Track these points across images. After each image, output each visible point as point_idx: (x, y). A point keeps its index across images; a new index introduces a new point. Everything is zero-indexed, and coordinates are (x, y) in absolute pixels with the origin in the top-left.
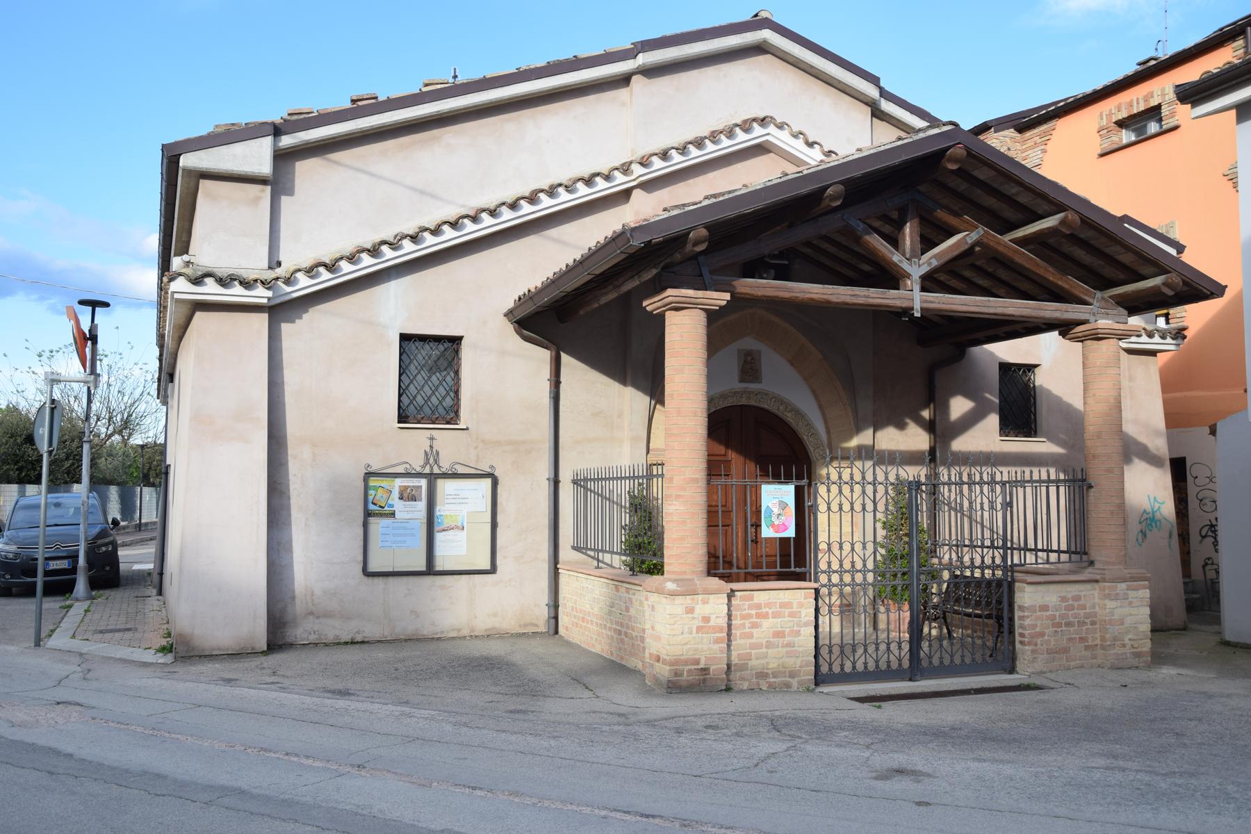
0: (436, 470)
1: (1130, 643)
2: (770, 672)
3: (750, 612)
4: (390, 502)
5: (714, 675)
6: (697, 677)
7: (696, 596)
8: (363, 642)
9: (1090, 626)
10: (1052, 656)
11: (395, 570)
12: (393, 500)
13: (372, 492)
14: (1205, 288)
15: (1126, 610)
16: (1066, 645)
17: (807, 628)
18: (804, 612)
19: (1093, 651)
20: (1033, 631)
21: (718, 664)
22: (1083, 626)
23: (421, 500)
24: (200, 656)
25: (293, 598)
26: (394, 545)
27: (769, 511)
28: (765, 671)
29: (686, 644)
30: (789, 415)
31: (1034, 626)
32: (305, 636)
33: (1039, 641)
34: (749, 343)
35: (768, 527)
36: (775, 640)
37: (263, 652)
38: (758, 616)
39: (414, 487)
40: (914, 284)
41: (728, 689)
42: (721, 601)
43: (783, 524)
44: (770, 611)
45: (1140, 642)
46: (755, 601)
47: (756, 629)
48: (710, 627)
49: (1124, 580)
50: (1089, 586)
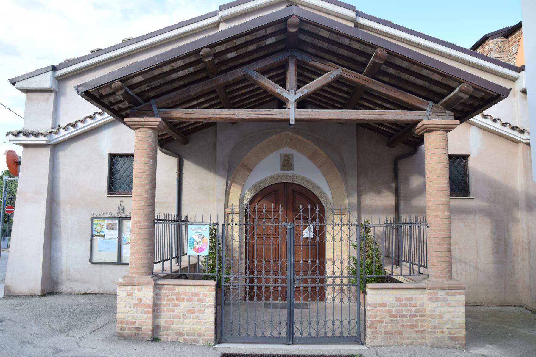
0: (123, 216)
1: (448, 330)
2: (185, 332)
3: (173, 297)
4: (102, 230)
5: (144, 331)
6: (134, 332)
7: (134, 287)
8: (91, 294)
9: (419, 318)
10: (388, 336)
11: (105, 262)
12: (104, 229)
13: (94, 226)
14: (492, 92)
15: (446, 309)
16: (399, 329)
17: (209, 309)
18: (207, 299)
19: (422, 334)
20: (374, 320)
21: (146, 326)
22: (413, 317)
23: (116, 230)
24: (14, 296)
25: (62, 272)
26: (104, 250)
27: (192, 240)
28: (182, 331)
29: (128, 313)
30: (310, 187)
31: (375, 316)
32: (66, 289)
33: (378, 326)
34: (287, 150)
35: (191, 249)
36: (188, 314)
37: (39, 296)
38: (178, 300)
39: (113, 223)
40: (292, 105)
41: (155, 339)
42: (149, 290)
43: (201, 247)
44: (186, 298)
45: (456, 330)
46: (177, 291)
47: (177, 307)
48: (142, 304)
49: (443, 289)
50: (419, 292)
